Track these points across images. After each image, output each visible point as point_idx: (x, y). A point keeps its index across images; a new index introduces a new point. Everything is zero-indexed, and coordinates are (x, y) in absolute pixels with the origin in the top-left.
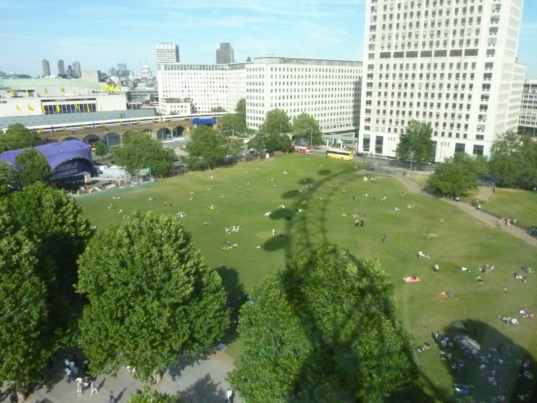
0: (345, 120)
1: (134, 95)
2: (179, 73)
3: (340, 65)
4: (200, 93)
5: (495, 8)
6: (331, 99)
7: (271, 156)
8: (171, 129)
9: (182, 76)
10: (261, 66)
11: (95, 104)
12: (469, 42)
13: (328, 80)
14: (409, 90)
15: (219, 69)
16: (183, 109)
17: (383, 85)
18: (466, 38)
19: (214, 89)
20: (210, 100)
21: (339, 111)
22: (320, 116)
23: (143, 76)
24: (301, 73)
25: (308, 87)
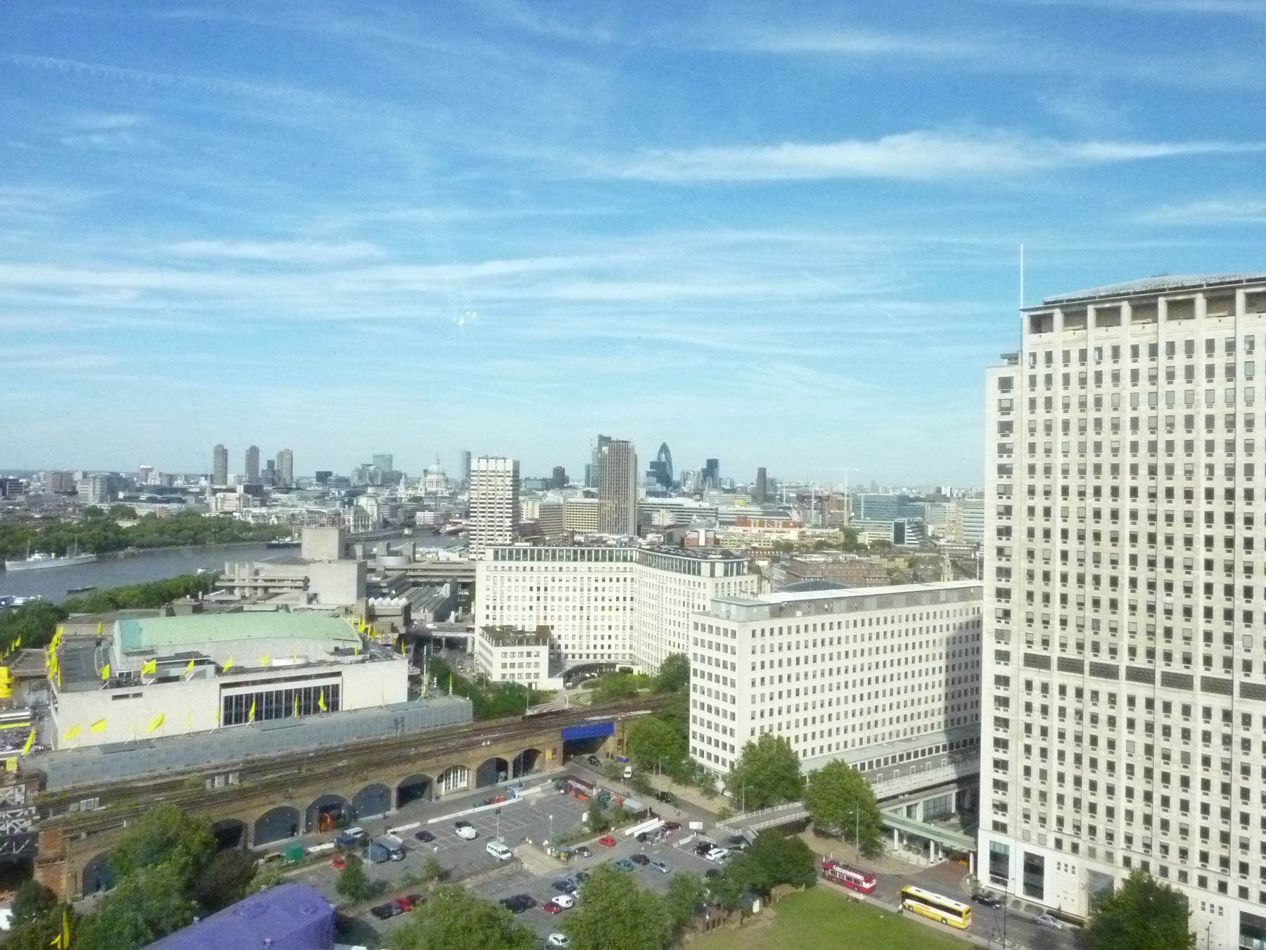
1: (413, 577)
4: (571, 613)
6: (888, 686)
7: (764, 904)
8: (509, 758)
10: (732, 626)
11: (337, 686)
13: (881, 643)
15: (618, 560)
16: (533, 660)
20: (592, 628)
21: (908, 711)
22: (865, 727)
23: (429, 489)
24: (819, 635)
25: (834, 664)
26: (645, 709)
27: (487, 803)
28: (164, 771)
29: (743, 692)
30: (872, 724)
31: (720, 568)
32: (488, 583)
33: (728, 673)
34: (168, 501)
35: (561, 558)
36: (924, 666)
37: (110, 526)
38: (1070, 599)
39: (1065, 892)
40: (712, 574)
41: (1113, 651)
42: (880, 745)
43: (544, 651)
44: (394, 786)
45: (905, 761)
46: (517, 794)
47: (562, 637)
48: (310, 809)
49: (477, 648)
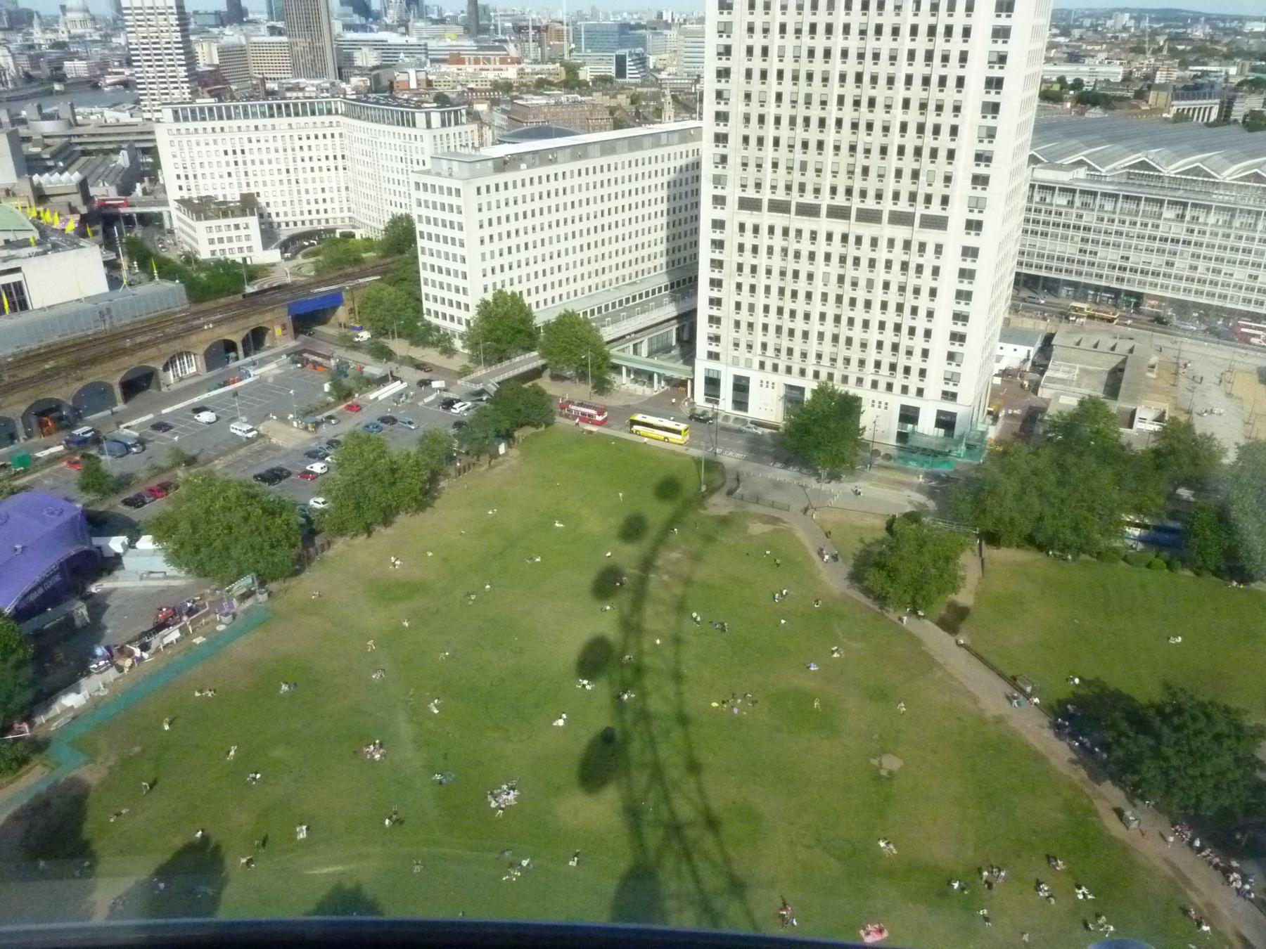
0: (646, 273)
1: (81, 144)
2: (213, 129)
3: (631, 149)
4: (277, 177)
7: (509, 446)
8: (237, 339)
9: (223, 135)
10: (455, 184)
12: (928, 199)
13: (605, 191)
14: (802, 286)
15: (321, 113)
16: (242, 232)
17: (747, 269)
18: (922, 189)
20: (303, 192)
22: (593, 275)
23: (73, 31)
24: (545, 187)
25: (561, 215)
26: (372, 275)
27: (224, 385)
29: (472, 251)
30: (600, 271)
31: (436, 118)
33: (456, 234)
35: (254, 115)
39: (766, 404)
40: (429, 126)
42: (608, 290)
43: (253, 221)
44: (115, 381)
45: (631, 304)
46: (252, 373)
47: (271, 204)
48: (25, 416)
49: (176, 224)
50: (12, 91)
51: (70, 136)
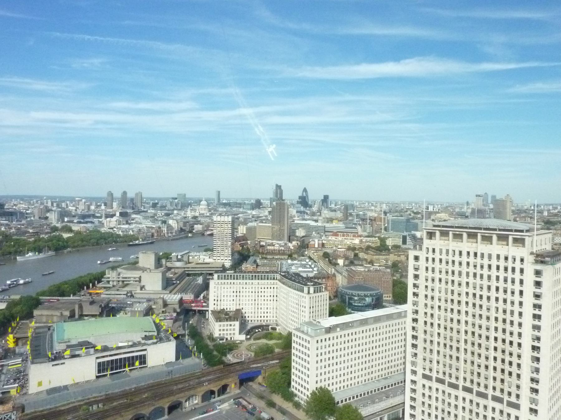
0: (393, 373)
1: (188, 271)
5: (534, 370)
8: (216, 389)
9: (234, 286)
10: (308, 338)
11: (145, 355)
12: (510, 394)
15: (271, 279)
16: (232, 327)
19: (264, 298)
20: (259, 308)
22: (367, 375)
23: (201, 212)
24: (347, 338)
28: (73, 400)
29: (313, 366)
30: (370, 373)
32: (215, 290)
34: (87, 222)
35: (246, 278)
36: (397, 339)
37: (60, 238)
38: (441, 353)
40: (309, 293)
41: (457, 378)
42: (374, 382)
44: (166, 406)
45: (384, 390)
46: (218, 408)
50: (174, 236)
51: (185, 268)
